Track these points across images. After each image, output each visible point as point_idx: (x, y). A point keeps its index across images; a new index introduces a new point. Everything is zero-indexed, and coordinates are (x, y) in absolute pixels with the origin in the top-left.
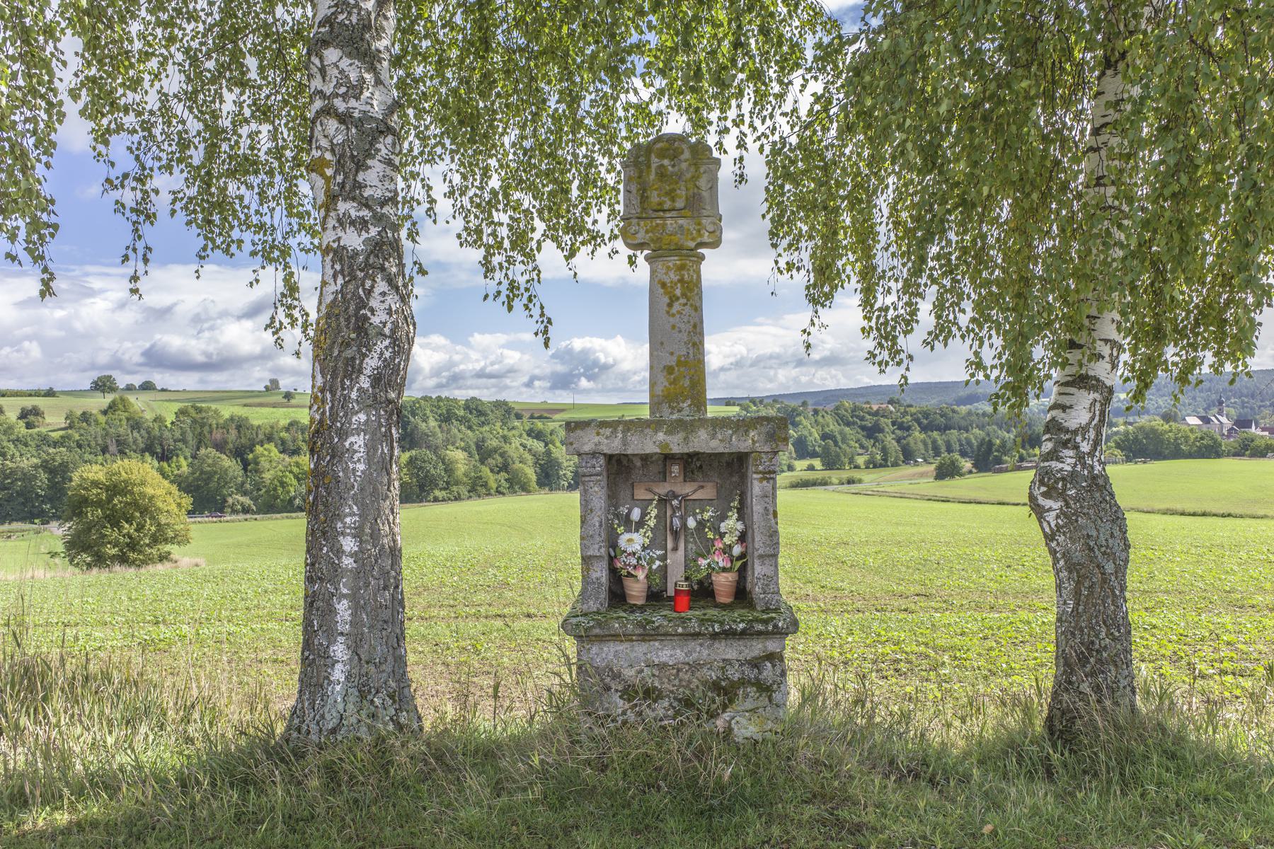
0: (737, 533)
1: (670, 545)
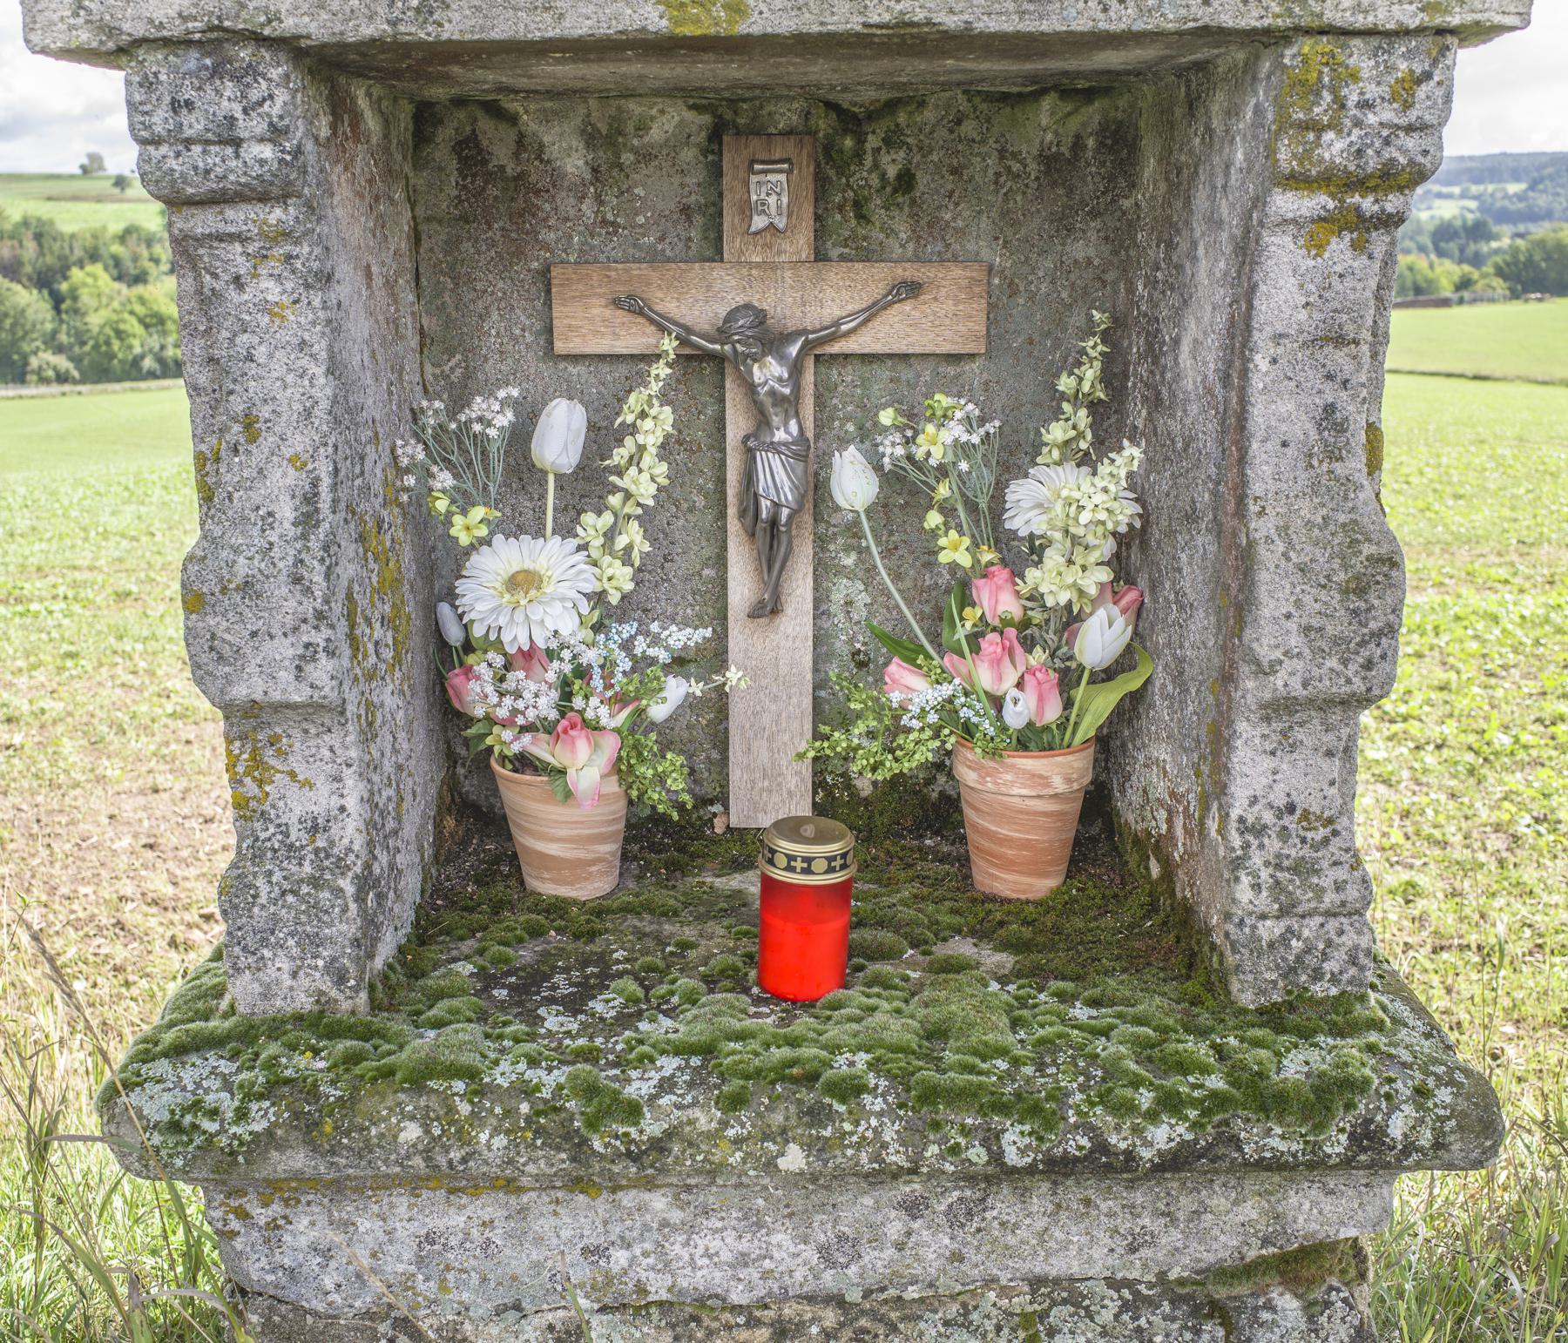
0: (1108, 547)
1: (742, 586)
